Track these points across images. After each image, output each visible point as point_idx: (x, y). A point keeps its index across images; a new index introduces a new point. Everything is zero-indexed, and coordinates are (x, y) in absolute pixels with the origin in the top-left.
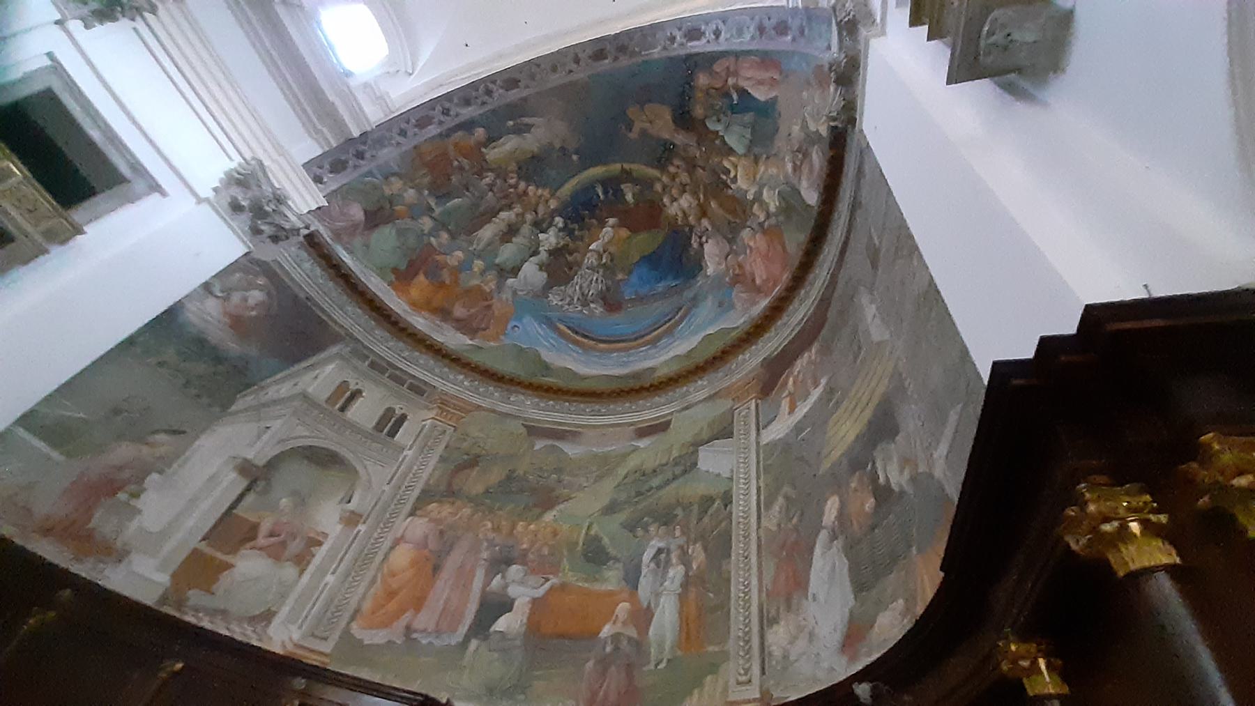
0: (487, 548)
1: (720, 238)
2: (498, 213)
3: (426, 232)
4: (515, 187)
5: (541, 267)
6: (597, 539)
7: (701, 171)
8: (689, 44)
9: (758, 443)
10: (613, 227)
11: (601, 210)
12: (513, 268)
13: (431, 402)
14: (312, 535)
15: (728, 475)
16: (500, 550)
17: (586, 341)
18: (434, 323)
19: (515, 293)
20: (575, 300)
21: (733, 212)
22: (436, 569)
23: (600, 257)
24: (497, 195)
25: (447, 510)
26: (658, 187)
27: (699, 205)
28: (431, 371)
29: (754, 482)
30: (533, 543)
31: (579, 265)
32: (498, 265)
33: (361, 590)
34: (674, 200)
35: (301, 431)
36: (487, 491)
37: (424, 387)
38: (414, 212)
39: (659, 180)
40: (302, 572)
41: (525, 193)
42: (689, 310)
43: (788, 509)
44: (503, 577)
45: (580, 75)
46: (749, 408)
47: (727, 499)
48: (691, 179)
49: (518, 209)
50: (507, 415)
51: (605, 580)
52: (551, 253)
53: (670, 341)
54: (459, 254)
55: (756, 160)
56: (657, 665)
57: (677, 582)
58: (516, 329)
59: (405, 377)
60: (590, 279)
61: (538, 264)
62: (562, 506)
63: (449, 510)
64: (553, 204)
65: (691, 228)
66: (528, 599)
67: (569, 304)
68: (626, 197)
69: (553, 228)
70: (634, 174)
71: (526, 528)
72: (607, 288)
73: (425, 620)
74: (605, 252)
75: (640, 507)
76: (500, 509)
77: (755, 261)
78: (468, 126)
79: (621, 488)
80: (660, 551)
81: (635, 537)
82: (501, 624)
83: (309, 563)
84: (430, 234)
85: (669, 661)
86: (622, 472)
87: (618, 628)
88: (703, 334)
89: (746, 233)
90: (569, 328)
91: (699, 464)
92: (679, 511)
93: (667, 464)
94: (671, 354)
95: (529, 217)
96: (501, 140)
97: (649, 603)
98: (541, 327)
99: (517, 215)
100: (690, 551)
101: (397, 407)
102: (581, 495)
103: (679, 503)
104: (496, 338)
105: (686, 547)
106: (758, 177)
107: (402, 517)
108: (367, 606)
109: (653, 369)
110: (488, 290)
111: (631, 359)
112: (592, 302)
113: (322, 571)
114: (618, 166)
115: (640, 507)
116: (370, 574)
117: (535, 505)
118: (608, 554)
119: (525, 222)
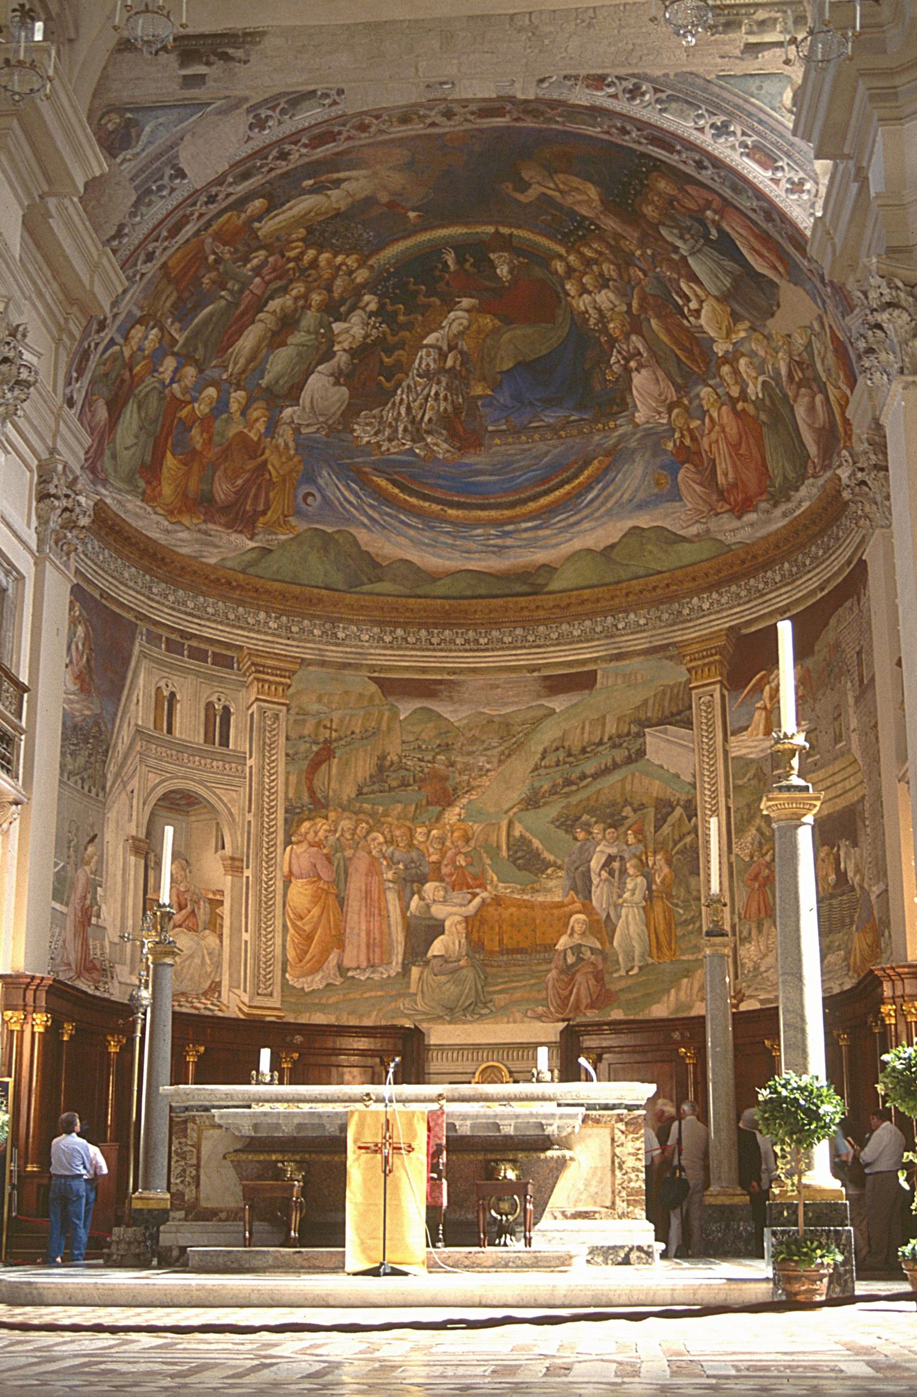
0: (389, 867)
1: (660, 374)
2: (265, 305)
3: (167, 381)
4: (298, 259)
5: (338, 377)
6: (523, 841)
7: (640, 274)
8: (650, 147)
9: (726, 752)
10: (467, 311)
11: (448, 284)
12: (292, 387)
13: (244, 675)
14: (211, 896)
15: (689, 779)
16: (406, 868)
17: (427, 504)
18: (199, 531)
19: (297, 430)
20: (401, 429)
21: (689, 352)
22: (342, 902)
23: (443, 356)
24: (267, 278)
25: (322, 826)
26: (560, 267)
27: (629, 312)
28: (226, 621)
29: (722, 799)
30: (443, 853)
31: (402, 368)
32: (268, 389)
33: (279, 941)
34: (584, 290)
35: (153, 778)
36: (360, 793)
37: (229, 653)
38: (156, 359)
39: (560, 257)
40: (221, 936)
41: (314, 264)
42: (606, 470)
43: (760, 844)
44: (422, 898)
45: (447, 127)
46: (712, 696)
47: (691, 810)
48: (620, 276)
49: (298, 288)
50: (345, 666)
51: (550, 891)
52: (352, 352)
53: (572, 520)
54: (211, 391)
55: (736, 317)
56: (627, 972)
57: (638, 896)
58: (310, 500)
59: (203, 646)
60: (425, 392)
61: (332, 375)
62: (464, 801)
63: (325, 827)
64: (361, 276)
65: (612, 341)
66: (458, 918)
67: (390, 440)
68: (498, 271)
69: (359, 312)
70: (515, 242)
72: (455, 409)
73: (353, 955)
74: (451, 348)
75: (574, 800)
76: (386, 814)
77: (717, 441)
78: (241, 203)
79: (543, 771)
80: (610, 859)
81: (576, 839)
82: (437, 948)
83: (222, 926)
84: (172, 381)
85: (641, 968)
86: (536, 747)
87: (577, 940)
88: (630, 524)
89: (705, 391)
90: (394, 483)
91: (648, 752)
92: (627, 812)
93: (601, 743)
94: (577, 544)
95: (316, 298)
96: (288, 205)
97: (608, 916)
98: (348, 487)
99: (296, 299)
100: (650, 863)
101: (214, 698)
102: (485, 781)
103: (626, 803)
104: (283, 523)
105: (644, 858)
106: (735, 338)
107: (279, 850)
108: (291, 955)
109: (548, 569)
110: (256, 439)
111: (509, 542)
112: (429, 432)
113: (236, 931)
114: (491, 229)
115: (574, 800)
116: (279, 923)
117: (428, 803)
118: (544, 860)
119: (310, 305)
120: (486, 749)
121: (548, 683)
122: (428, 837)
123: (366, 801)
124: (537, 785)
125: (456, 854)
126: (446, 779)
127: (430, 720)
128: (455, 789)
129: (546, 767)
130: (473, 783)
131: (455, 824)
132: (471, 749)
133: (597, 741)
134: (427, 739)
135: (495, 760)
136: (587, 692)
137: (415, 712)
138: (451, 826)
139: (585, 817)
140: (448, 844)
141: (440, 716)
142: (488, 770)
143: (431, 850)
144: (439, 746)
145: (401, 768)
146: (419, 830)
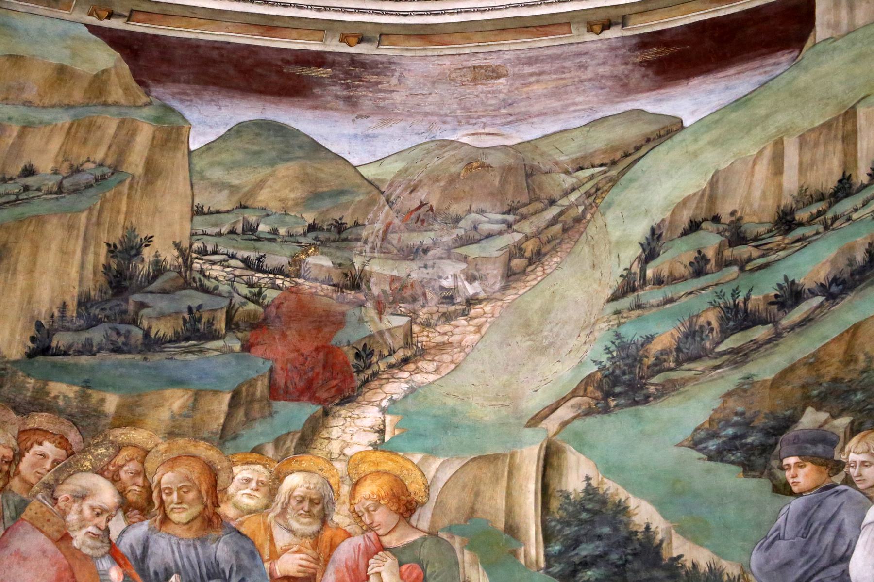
71: (272, 488)
120: (465, 241)
121: (652, 53)
122: (272, 493)
123: (64, 373)
124: (632, 332)
125: (369, 555)
126: (339, 323)
127: (284, 156)
128: (365, 354)
129: (659, 281)
130: (423, 338)
131: (362, 457)
132: (417, 239)
133: (831, 184)
134: (274, 206)
135: (494, 273)
136: (784, 58)
137: (239, 130)
138: (353, 462)
139: (811, 419)
140: (340, 517)
141: (316, 148)
142: (471, 302)
143: (282, 538)
144: (312, 228)
145: (186, 285)
146: (241, 472)
